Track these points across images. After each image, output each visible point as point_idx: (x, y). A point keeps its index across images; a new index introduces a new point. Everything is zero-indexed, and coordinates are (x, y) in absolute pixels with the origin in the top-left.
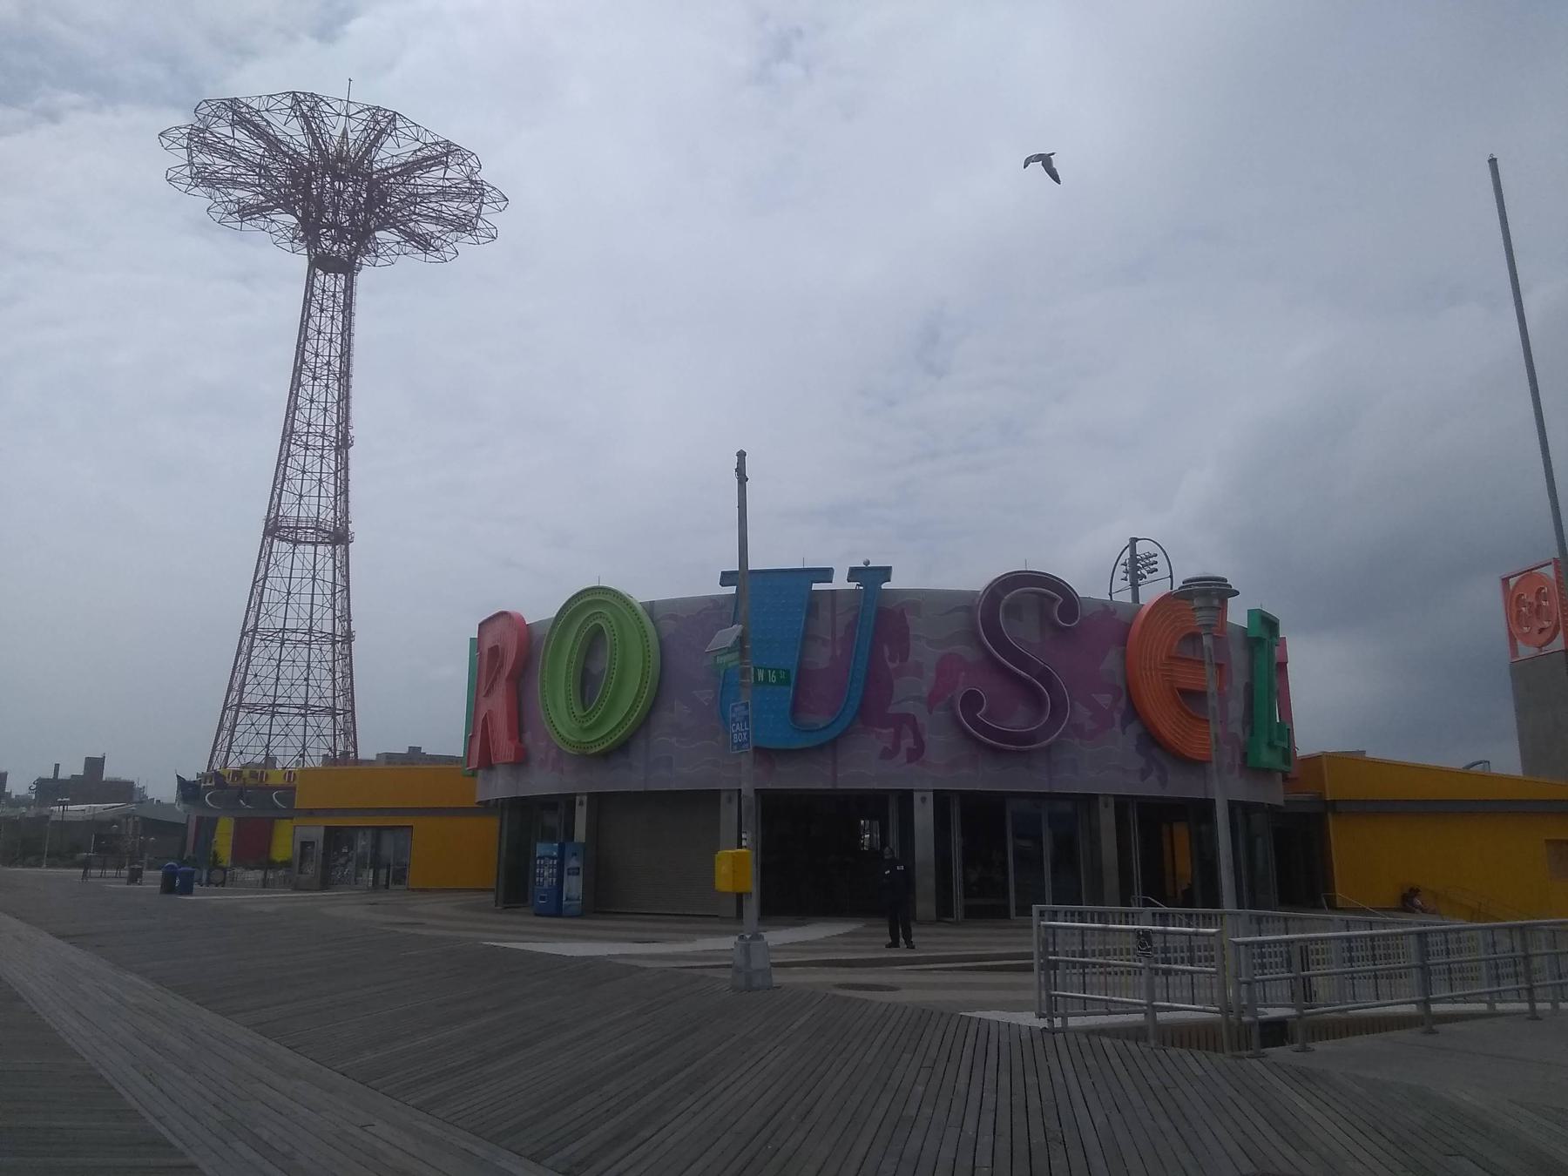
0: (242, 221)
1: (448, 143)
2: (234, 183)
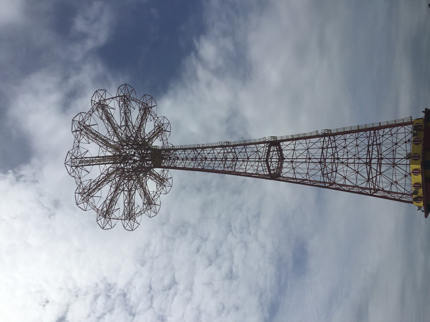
0: (155, 204)
2: (130, 202)
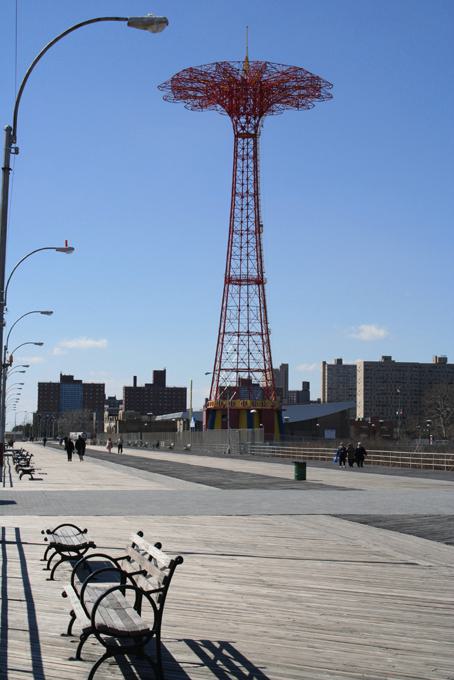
1: (295, 67)
